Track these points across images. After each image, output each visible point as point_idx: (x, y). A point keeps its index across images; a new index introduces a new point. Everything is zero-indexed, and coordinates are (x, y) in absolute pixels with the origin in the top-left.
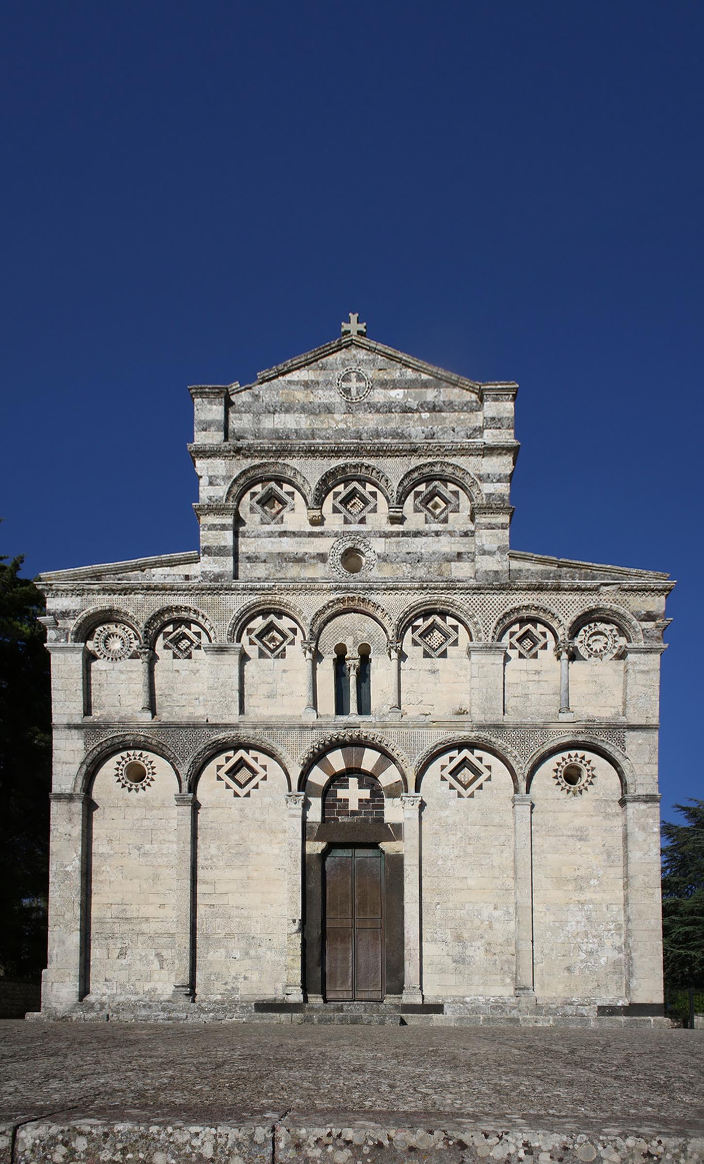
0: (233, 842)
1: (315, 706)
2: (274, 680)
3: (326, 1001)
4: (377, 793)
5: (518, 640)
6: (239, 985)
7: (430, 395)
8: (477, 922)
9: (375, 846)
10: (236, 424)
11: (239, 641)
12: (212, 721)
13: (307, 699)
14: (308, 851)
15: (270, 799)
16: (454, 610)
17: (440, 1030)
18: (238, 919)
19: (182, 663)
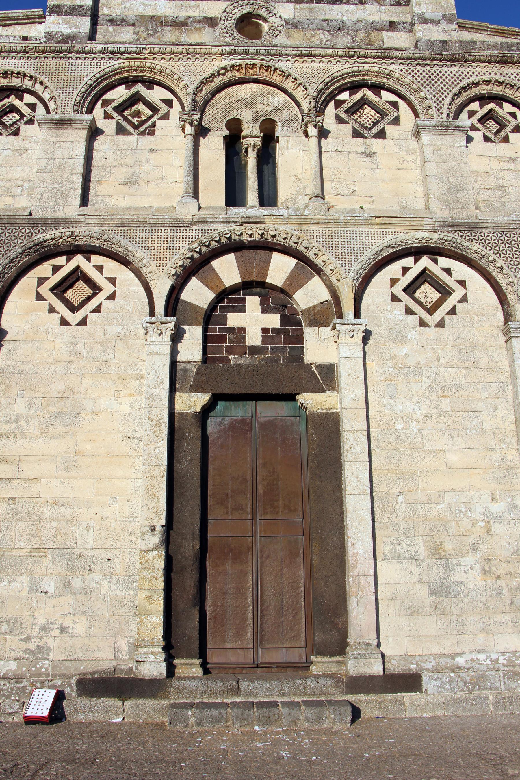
0: (54, 394)
1: (196, 195)
2: (137, 162)
3: (206, 671)
4: (291, 320)
5: (479, 121)
6: (50, 643)
8: (465, 523)
9: (291, 397)
11: (90, 111)
12: (38, 214)
14: (179, 408)
15: (119, 329)
16: (391, 83)
17: (419, 727)
18: (54, 524)
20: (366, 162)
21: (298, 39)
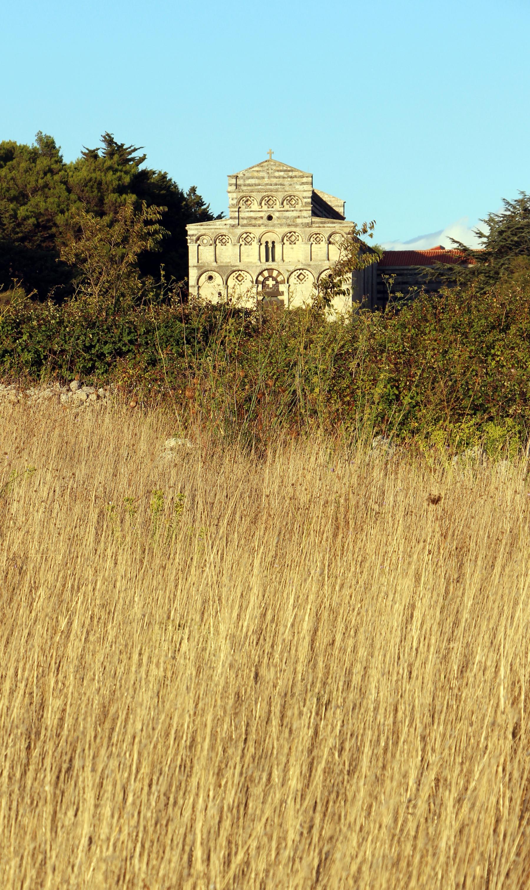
7: (290, 174)
10: (238, 183)
13: (258, 257)
19: (223, 247)
20: (291, 250)
21: (279, 222)
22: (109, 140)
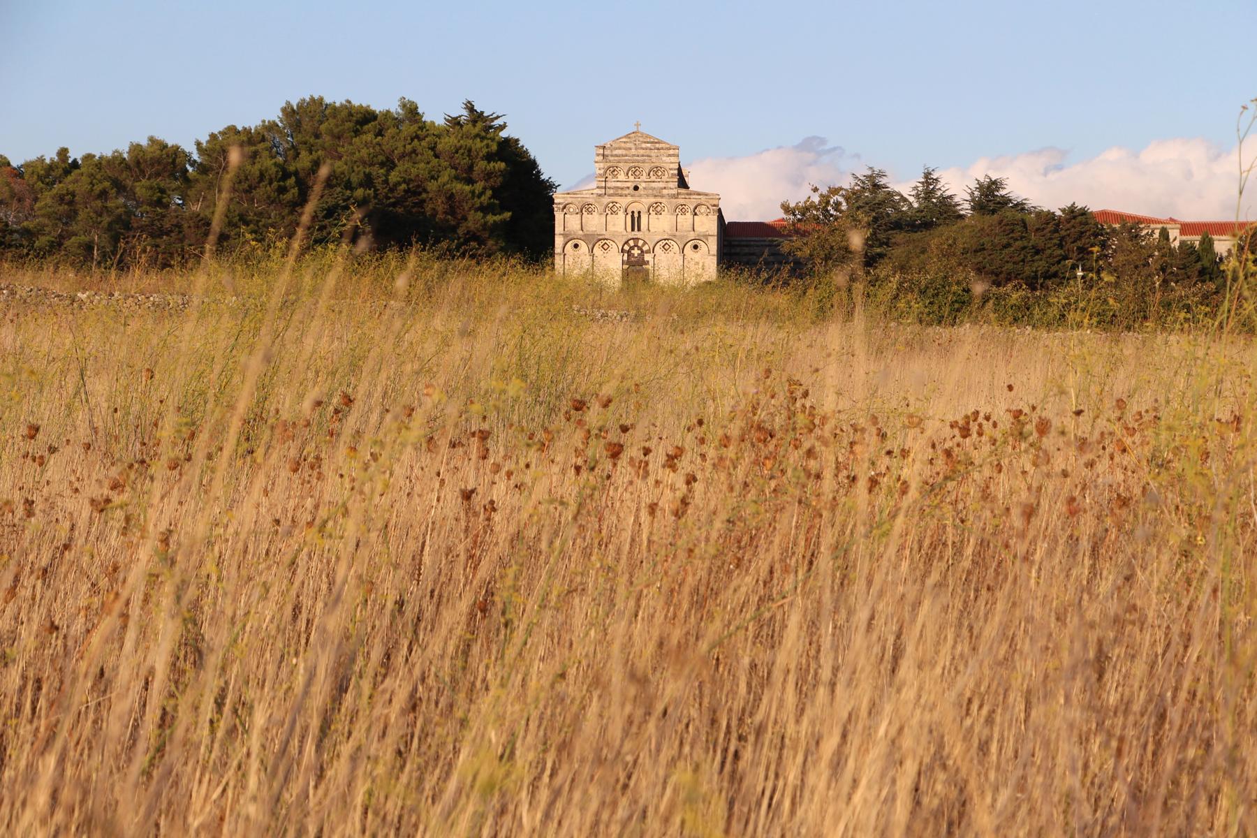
22: (470, 107)
